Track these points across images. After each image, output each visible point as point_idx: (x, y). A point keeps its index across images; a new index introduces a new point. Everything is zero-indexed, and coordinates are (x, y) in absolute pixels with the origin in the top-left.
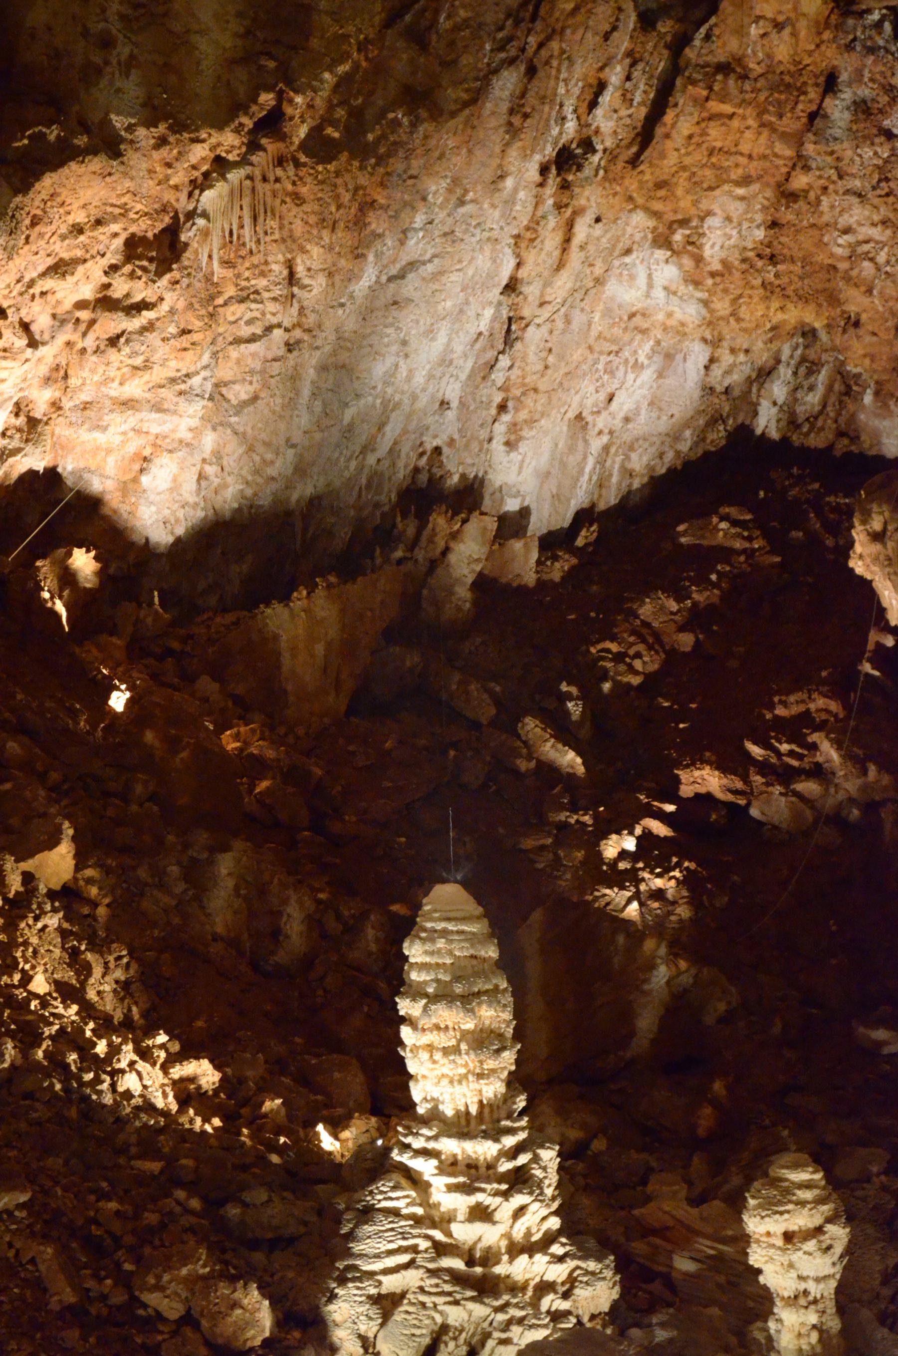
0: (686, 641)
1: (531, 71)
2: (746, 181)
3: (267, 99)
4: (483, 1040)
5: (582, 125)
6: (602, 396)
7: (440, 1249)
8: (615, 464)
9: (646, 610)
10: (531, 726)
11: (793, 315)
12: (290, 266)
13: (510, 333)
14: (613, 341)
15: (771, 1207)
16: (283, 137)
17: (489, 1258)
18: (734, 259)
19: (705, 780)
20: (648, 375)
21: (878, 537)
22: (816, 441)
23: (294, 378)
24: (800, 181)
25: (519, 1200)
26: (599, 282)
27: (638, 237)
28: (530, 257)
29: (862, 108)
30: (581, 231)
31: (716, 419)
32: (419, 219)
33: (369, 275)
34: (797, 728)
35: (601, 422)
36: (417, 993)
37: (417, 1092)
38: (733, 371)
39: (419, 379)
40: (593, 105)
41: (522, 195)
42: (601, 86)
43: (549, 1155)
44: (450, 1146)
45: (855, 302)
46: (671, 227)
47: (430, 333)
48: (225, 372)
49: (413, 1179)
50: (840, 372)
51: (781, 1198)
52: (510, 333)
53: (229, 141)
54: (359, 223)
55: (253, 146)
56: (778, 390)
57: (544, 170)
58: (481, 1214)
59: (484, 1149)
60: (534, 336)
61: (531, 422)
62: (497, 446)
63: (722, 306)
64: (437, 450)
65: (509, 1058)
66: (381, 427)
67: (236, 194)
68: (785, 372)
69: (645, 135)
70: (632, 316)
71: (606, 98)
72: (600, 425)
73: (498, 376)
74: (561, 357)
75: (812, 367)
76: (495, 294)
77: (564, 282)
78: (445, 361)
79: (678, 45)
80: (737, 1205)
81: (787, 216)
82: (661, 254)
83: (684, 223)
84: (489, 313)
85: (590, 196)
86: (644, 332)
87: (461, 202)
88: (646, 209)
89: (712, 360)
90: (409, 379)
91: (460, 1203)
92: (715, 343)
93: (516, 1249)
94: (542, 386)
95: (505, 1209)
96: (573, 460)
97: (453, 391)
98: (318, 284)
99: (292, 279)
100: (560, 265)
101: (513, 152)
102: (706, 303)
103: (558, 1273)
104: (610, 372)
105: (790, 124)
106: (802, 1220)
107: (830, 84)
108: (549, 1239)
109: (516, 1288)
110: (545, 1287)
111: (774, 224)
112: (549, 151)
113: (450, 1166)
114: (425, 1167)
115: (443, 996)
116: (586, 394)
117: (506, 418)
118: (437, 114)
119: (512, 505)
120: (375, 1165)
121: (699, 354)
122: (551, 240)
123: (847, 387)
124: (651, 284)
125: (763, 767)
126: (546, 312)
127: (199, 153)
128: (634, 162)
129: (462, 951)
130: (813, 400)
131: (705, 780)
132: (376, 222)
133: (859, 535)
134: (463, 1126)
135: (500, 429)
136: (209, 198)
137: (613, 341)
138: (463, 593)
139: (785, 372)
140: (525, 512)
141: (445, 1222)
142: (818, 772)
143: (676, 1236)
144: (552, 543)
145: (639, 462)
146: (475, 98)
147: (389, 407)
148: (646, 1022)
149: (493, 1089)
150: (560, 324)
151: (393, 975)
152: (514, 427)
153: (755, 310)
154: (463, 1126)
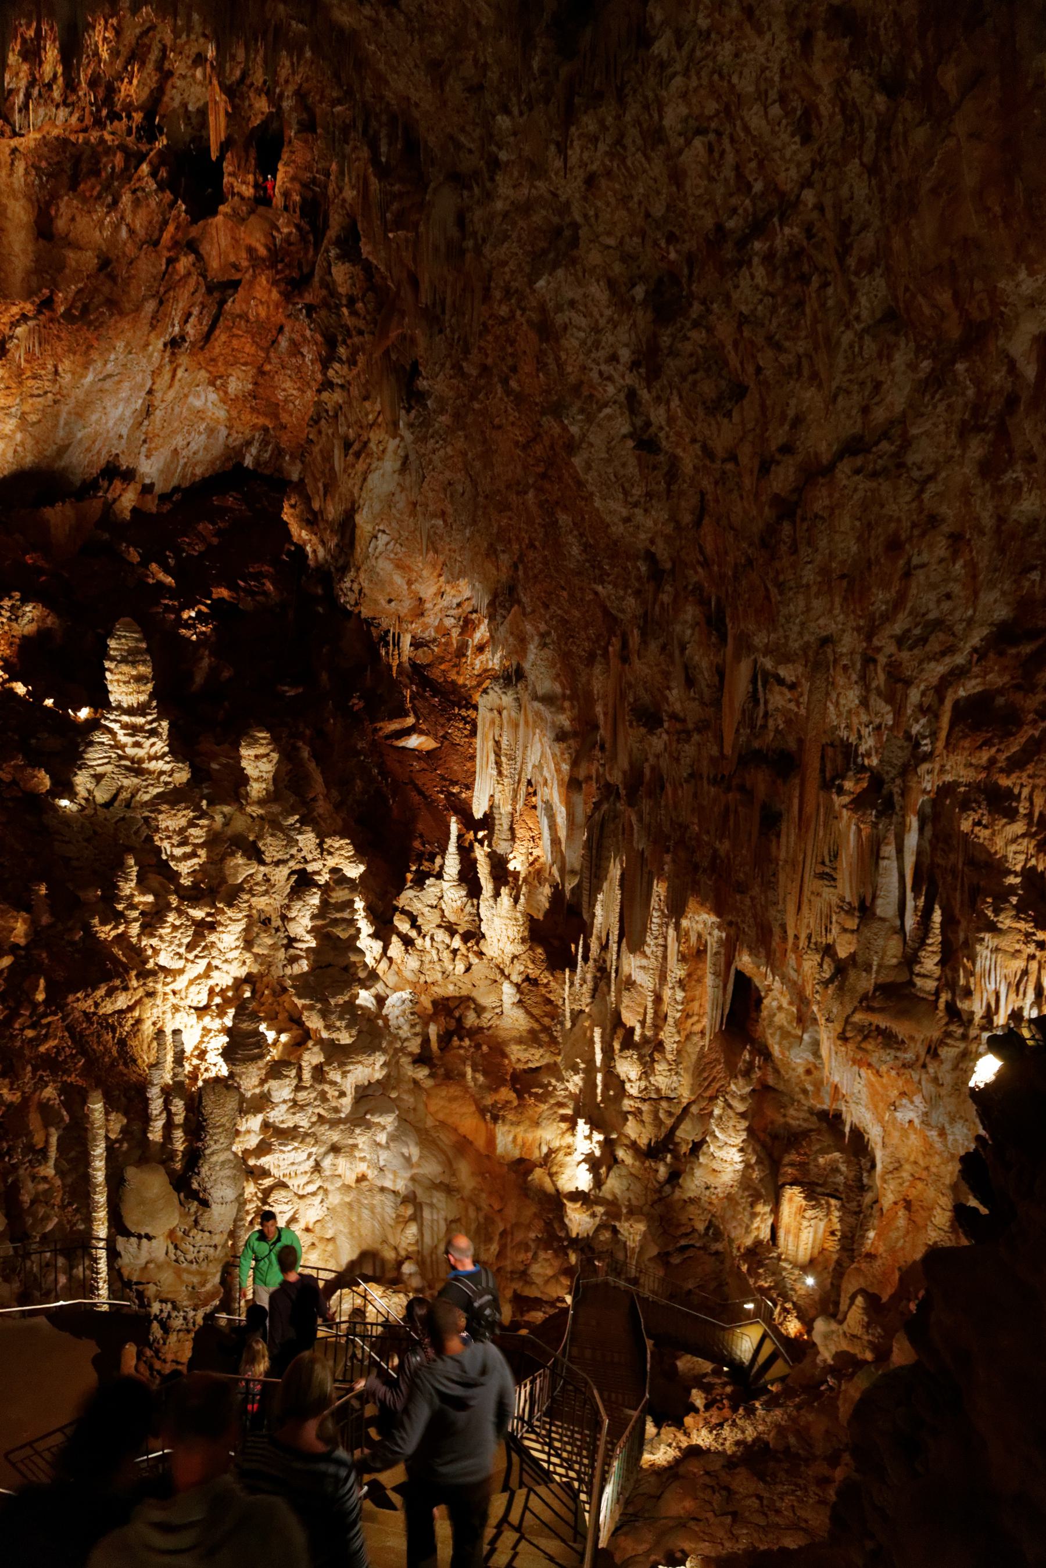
0: (215, 541)
1: (161, 303)
2: (245, 364)
3: (46, 291)
4: (139, 679)
5: (182, 329)
7: (120, 758)
9: (201, 527)
10: (154, 567)
11: (261, 421)
12: (56, 367)
13: (148, 411)
15: (250, 745)
16: (53, 310)
17: (141, 761)
19: (224, 593)
20: (204, 437)
21: (293, 506)
22: (267, 472)
23: (57, 416)
24: (267, 368)
25: (153, 740)
26: (186, 396)
28: (158, 380)
29: (293, 343)
30: (180, 373)
31: (229, 459)
32: (112, 357)
33: (90, 377)
34: (258, 576)
36: (112, 659)
37: (112, 698)
38: (236, 439)
39: (111, 424)
40: (186, 321)
42: (190, 315)
43: (165, 724)
44: (125, 718)
45: (285, 418)
46: (216, 378)
47: (116, 406)
48: (26, 408)
49: (110, 731)
50: (277, 447)
51: (254, 742)
52: (148, 411)
53: (29, 308)
54: (86, 353)
55: (39, 312)
56: (254, 451)
57: (165, 345)
58: (137, 745)
59: (140, 720)
60: (159, 414)
62: (142, 457)
63: (234, 414)
65: (150, 686)
67: (31, 331)
68: (256, 444)
69: (207, 337)
71: (192, 320)
75: (267, 444)
76: (143, 394)
77: (171, 394)
78: (121, 419)
79: (222, 303)
80: (236, 747)
81: (261, 381)
85: (184, 360)
91: (129, 740)
93: (151, 758)
95: (147, 743)
97: (124, 432)
98: (68, 377)
99: (56, 372)
100: (170, 386)
101: (153, 335)
103: (167, 767)
105: (265, 344)
106: (262, 751)
107: (281, 329)
108: (164, 755)
109: (150, 772)
110: (162, 773)
111: (256, 384)
112: (168, 338)
113: (125, 726)
114: (115, 727)
115: (124, 661)
116: (179, 441)
118: (122, 313)
119: (147, 481)
120: (93, 725)
121: (223, 432)
122: (167, 376)
123: (279, 452)
124: (206, 400)
125: (244, 589)
127: (15, 310)
128: (202, 348)
129: (132, 644)
130: (267, 455)
131: (224, 593)
132: (94, 355)
133: (286, 505)
134: (130, 711)
135: (143, 449)
136: (19, 331)
138: (127, 515)
139: (256, 444)
140: (152, 485)
141: (123, 747)
142: (265, 593)
143: (214, 757)
144: (163, 498)
145: (198, 471)
146: (138, 308)
148: (199, 679)
149: (143, 698)
151: (103, 653)
152: (149, 450)
153: (246, 417)
154: (130, 711)
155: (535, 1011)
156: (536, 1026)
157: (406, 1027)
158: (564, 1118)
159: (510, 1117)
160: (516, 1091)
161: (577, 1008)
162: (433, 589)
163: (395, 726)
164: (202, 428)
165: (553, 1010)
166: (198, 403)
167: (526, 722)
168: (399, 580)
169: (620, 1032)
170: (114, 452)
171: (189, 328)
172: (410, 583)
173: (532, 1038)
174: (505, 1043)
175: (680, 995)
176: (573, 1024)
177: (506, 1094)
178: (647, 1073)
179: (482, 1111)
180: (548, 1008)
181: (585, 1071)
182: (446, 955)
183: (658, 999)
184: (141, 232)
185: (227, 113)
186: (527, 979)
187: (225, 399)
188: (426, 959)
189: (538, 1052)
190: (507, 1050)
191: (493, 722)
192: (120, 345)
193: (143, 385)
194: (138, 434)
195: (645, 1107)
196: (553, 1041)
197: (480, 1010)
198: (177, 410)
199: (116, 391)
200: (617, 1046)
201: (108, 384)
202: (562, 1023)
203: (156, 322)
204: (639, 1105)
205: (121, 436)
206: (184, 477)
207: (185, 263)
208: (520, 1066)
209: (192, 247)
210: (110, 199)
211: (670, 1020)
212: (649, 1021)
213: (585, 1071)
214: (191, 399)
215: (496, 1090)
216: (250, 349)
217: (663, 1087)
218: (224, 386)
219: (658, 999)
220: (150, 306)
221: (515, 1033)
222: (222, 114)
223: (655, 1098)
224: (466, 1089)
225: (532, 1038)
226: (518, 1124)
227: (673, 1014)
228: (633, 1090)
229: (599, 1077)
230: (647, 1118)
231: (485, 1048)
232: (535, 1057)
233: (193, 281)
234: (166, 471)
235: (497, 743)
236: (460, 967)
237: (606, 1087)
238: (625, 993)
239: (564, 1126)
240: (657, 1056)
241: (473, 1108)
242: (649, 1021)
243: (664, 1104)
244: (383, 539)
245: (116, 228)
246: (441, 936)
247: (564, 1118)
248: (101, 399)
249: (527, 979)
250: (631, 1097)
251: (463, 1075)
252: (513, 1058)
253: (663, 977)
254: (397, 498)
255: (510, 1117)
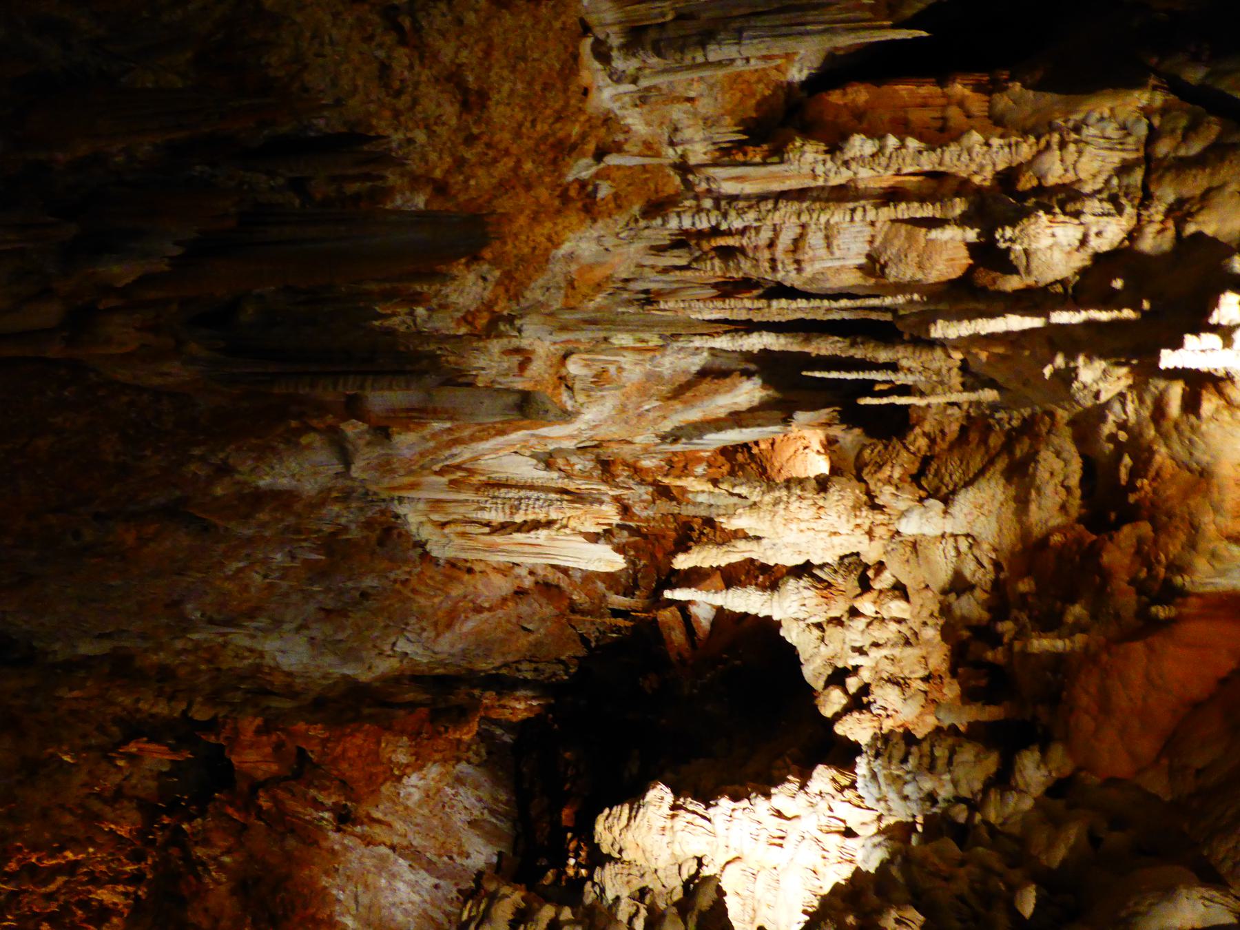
1: (292, 831)
2: (379, 743)
5: (328, 810)
6: (464, 812)
8: (502, 808)
14: (436, 805)
18: (412, 750)
20: (462, 790)
26: (407, 808)
27: (392, 789)
30: (377, 815)
32: (334, 892)
35: (476, 813)
39: (416, 898)
41: (346, 842)
47: (394, 891)
57: (338, 830)
61: (460, 846)
63: (437, 756)
64: (459, 891)
66: (432, 919)
70: (428, 796)
71: (321, 798)
72: (478, 813)
73: (435, 859)
74: (431, 830)
77: (399, 826)
78: (413, 885)
82: (405, 780)
83: (392, 770)
84: (401, 861)
85: (361, 812)
86: (439, 790)
87: (337, 870)
88: (382, 784)
89: (469, 762)
90: (412, 903)
92: (459, 760)
94: (442, 839)
96: (488, 827)
100: (390, 825)
101: (325, 844)
102: (435, 762)
104: (452, 807)
111: (402, 733)
116: (459, 819)
117: (455, 856)
119: (495, 859)
121: (463, 767)
122: (377, 830)
124: (414, 786)
126: (411, 835)
135: (458, 860)
137: (436, 805)
145: (503, 797)
147: (425, 916)
150: (417, 829)
152: (460, 854)
155: (976, 463)
156: (1001, 464)
157: (927, 784)
158: (1191, 404)
159: (1175, 548)
160: (1117, 526)
161: (956, 379)
162: (497, 579)
163: (678, 636)
164: (450, 791)
165: (976, 425)
166: (417, 796)
167: (413, 486)
168: (471, 624)
169: (984, 277)
170: (454, 894)
171: (329, 802)
172: (479, 610)
173: (1020, 475)
174: (1025, 534)
175: (860, 145)
176: (992, 384)
177: (1118, 554)
178: (1065, 199)
179: (1148, 627)
180: (974, 436)
181: (1071, 356)
182: (878, 634)
183: (891, 196)
184: (231, 841)
185: (149, 742)
186: (916, 479)
187: (419, 763)
188: (888, 669)
189: (1048, 462)
190: (1037, 532)
191: (463, 535)
192: (325, 881)
193: (383, 859)
194: (440, 865)
195: (1167, 194)
196: (1029, 427)
197: (959, 585)
198: (419, 820)
199: (378, 889)
200: (1013, 283)
201: (365, 899)
202: (994, 407)
203: (310, 836)
204: (1157, 211)
205: (436, 886)
206: (506, 815)
207: (265, 803)
208: (1075, 502)
209: (256, 786)
210: (200, 868)
211: (928, 162)
212: (928, 211)
213: (1071, 356)
214: (410, 803)
215: (1106, 575)
216: (359, 740)
217: (1115, 158)
218: (399, 766)
219: (891, 196)
220: (291, 843)
221: (1009, 511)
222: (147, 746)
223: (1147, 170)
224: (1088, 657)
225: (1020, 475)
226: (1194, 528)
227: (912, 158)
228: (1110, 232)
229: (1062, 317)
230: (1195, 184)
231: (1024, 586)
232: (1059, 469)
233: (281, 794)
234: (491, 835)
235: (504, 528)
236: (897, 608)
237: (1108, 300)
238: (893, 274)
239: (1209, 404)
240: (1027, 182)
241: (1139, 646)
242: (928, 211)
243: (1163, 148)
244: (403, 646)
245: (222, 867)
246: (856, 633)
247: (1191, 404)
248: (381, 908)
249: (916, 479)
250: (1133, 235)
251: (1058, 659)
252: (1057, 520)
253: (843, 194)
254: (314, 633)
255: (1175, 548)
